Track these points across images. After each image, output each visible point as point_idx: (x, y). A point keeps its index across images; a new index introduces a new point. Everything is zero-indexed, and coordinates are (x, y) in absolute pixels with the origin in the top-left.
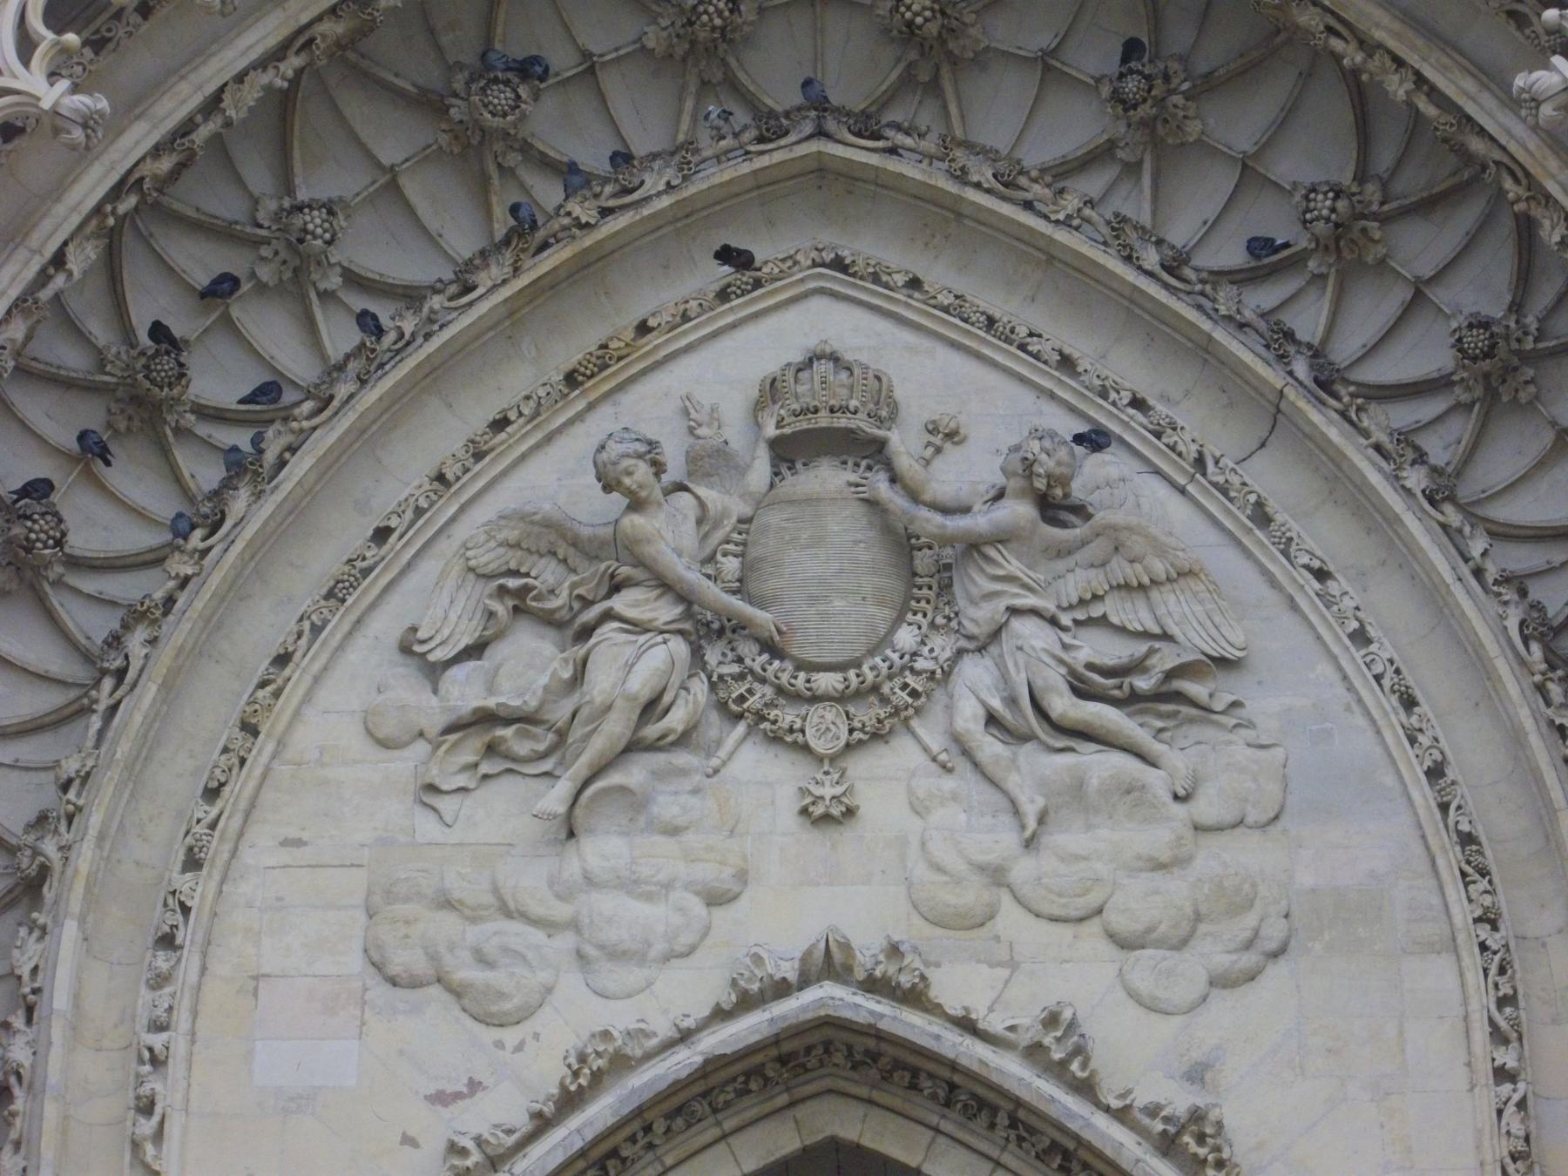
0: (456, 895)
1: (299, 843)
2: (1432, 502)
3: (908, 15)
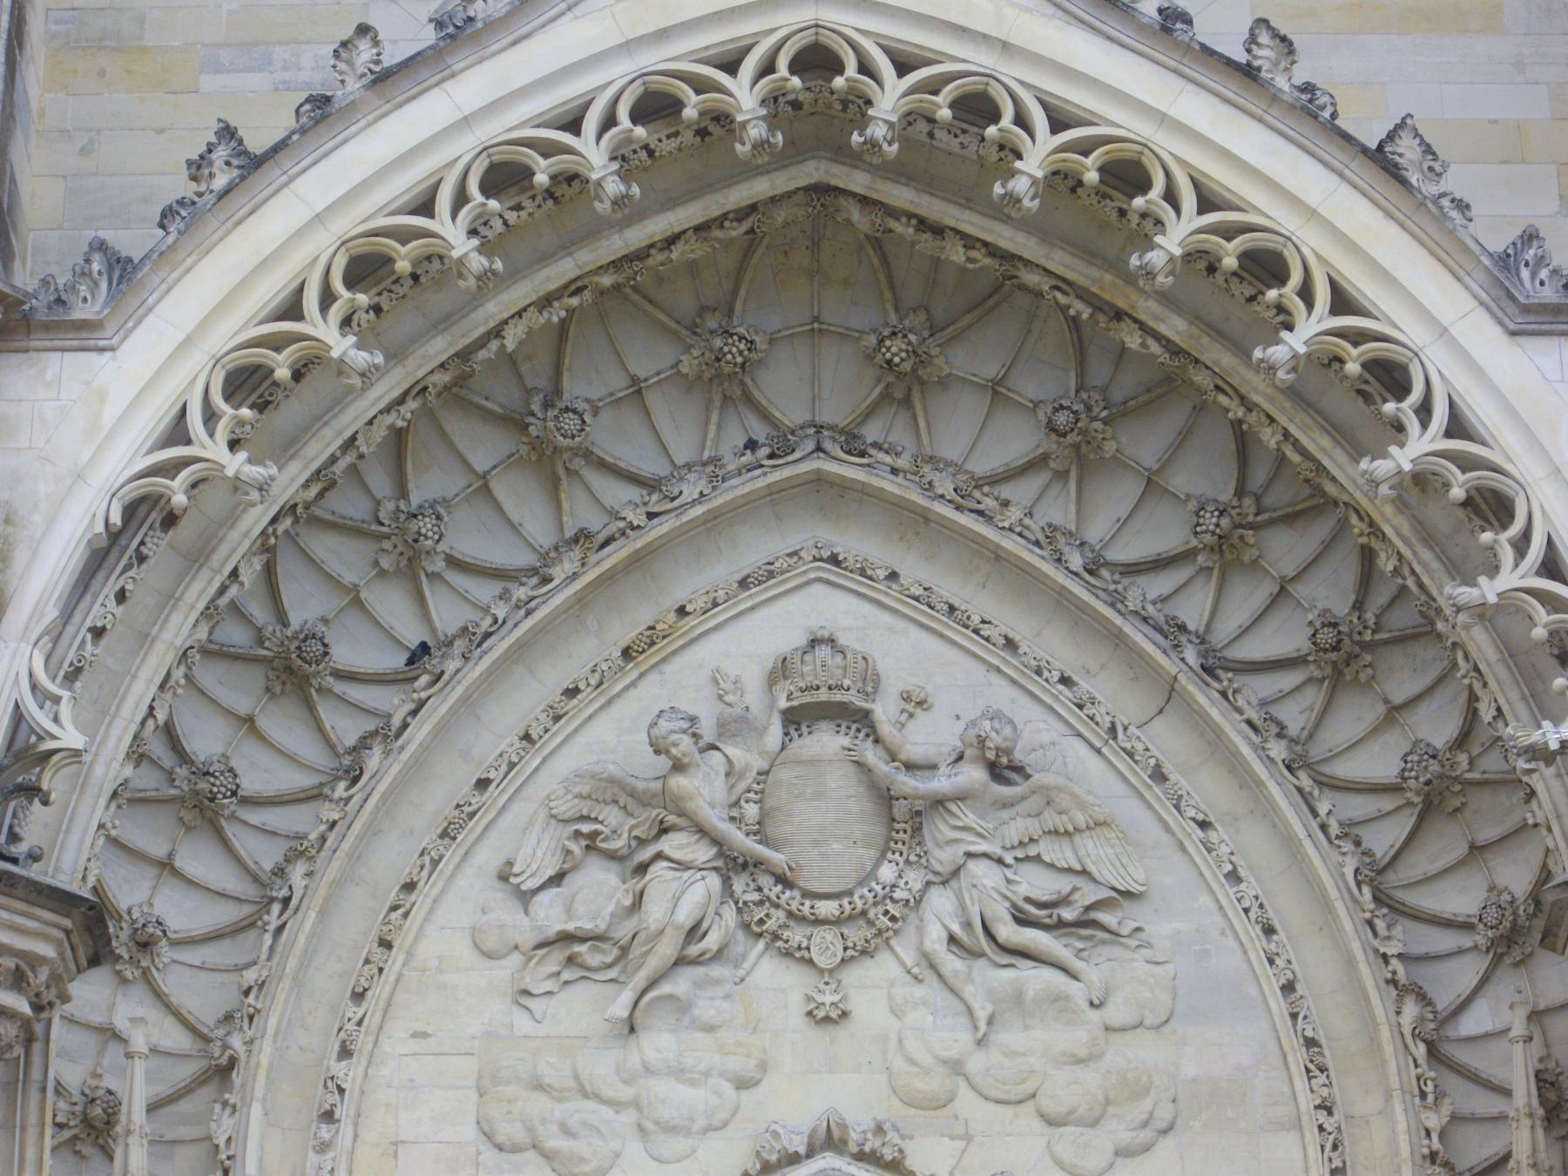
0: (547, 1080)
1: (424, 1035)
2: (1289, 768)
3: (888, 355)
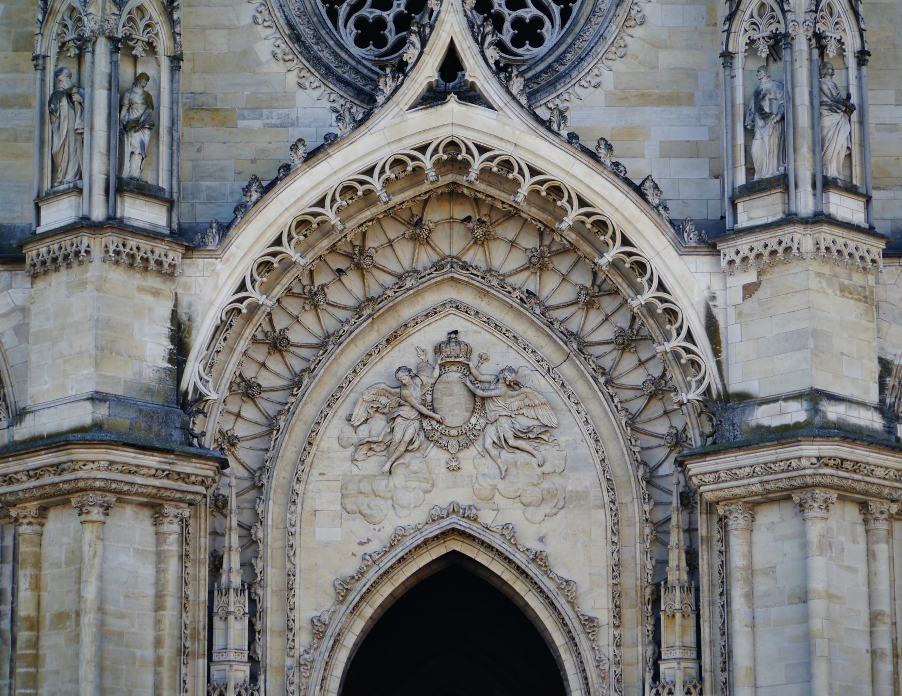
1: (323, 474)
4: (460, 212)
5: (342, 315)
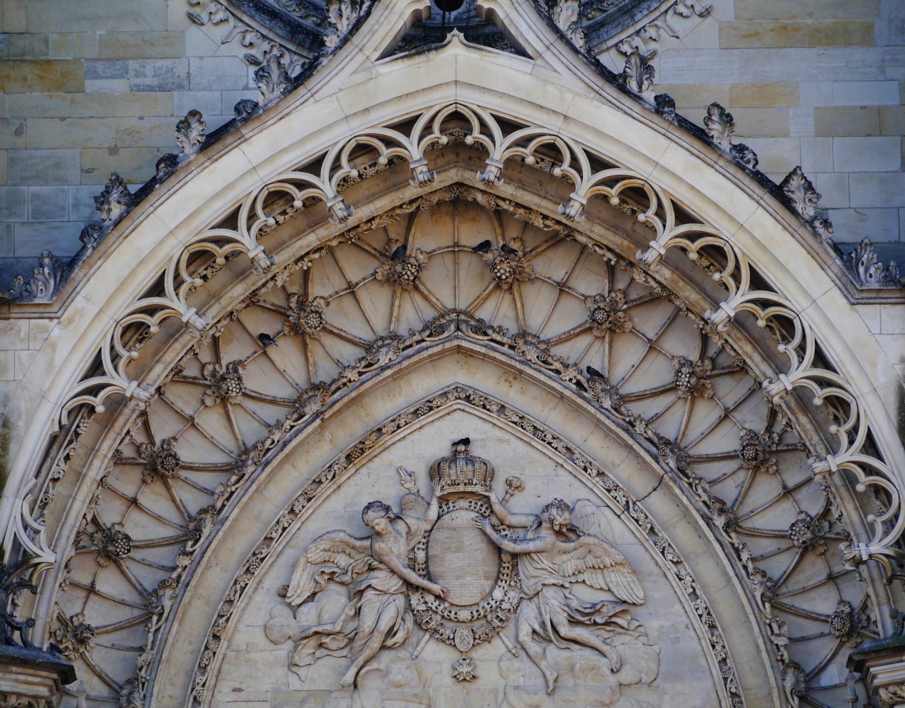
3: (498, 274)
4: (472, 234)
5: (270, 413)
